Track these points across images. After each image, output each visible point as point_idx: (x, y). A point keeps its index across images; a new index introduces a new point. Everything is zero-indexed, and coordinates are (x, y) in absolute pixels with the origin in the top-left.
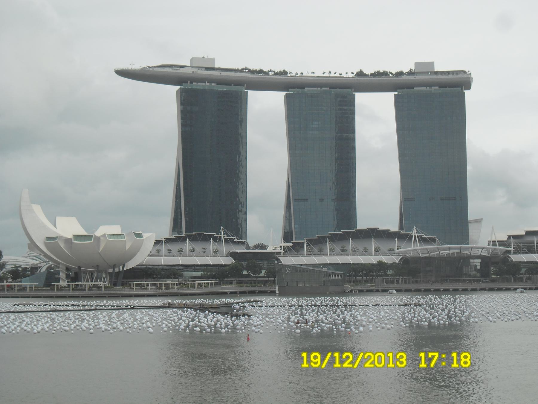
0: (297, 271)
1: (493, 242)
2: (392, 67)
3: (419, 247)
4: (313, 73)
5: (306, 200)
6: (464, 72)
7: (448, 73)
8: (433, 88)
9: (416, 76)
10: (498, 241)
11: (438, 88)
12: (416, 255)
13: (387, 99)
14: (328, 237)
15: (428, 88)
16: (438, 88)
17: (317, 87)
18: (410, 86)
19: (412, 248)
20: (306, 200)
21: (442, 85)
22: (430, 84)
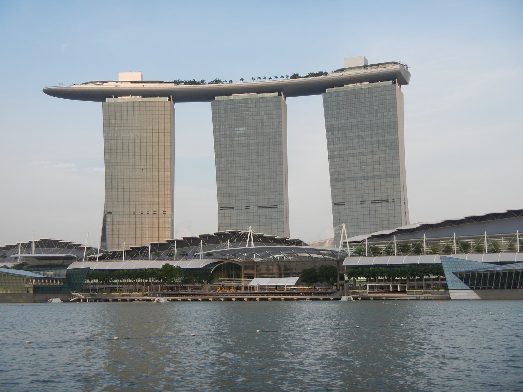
2: (330, 66)
4: (242, 80)
5: (232, 208)
6: (395, 63)
7: (377, 65)
8: (363, 83)
9: (343, 73)
11: (368, 83)
12: (247, 260)
13: (316, 101)
14: (178, 241)
15: (359, 84)
16: (368, 83)
17: (244, 93)
20: (232, 208)
21: (373, 79)
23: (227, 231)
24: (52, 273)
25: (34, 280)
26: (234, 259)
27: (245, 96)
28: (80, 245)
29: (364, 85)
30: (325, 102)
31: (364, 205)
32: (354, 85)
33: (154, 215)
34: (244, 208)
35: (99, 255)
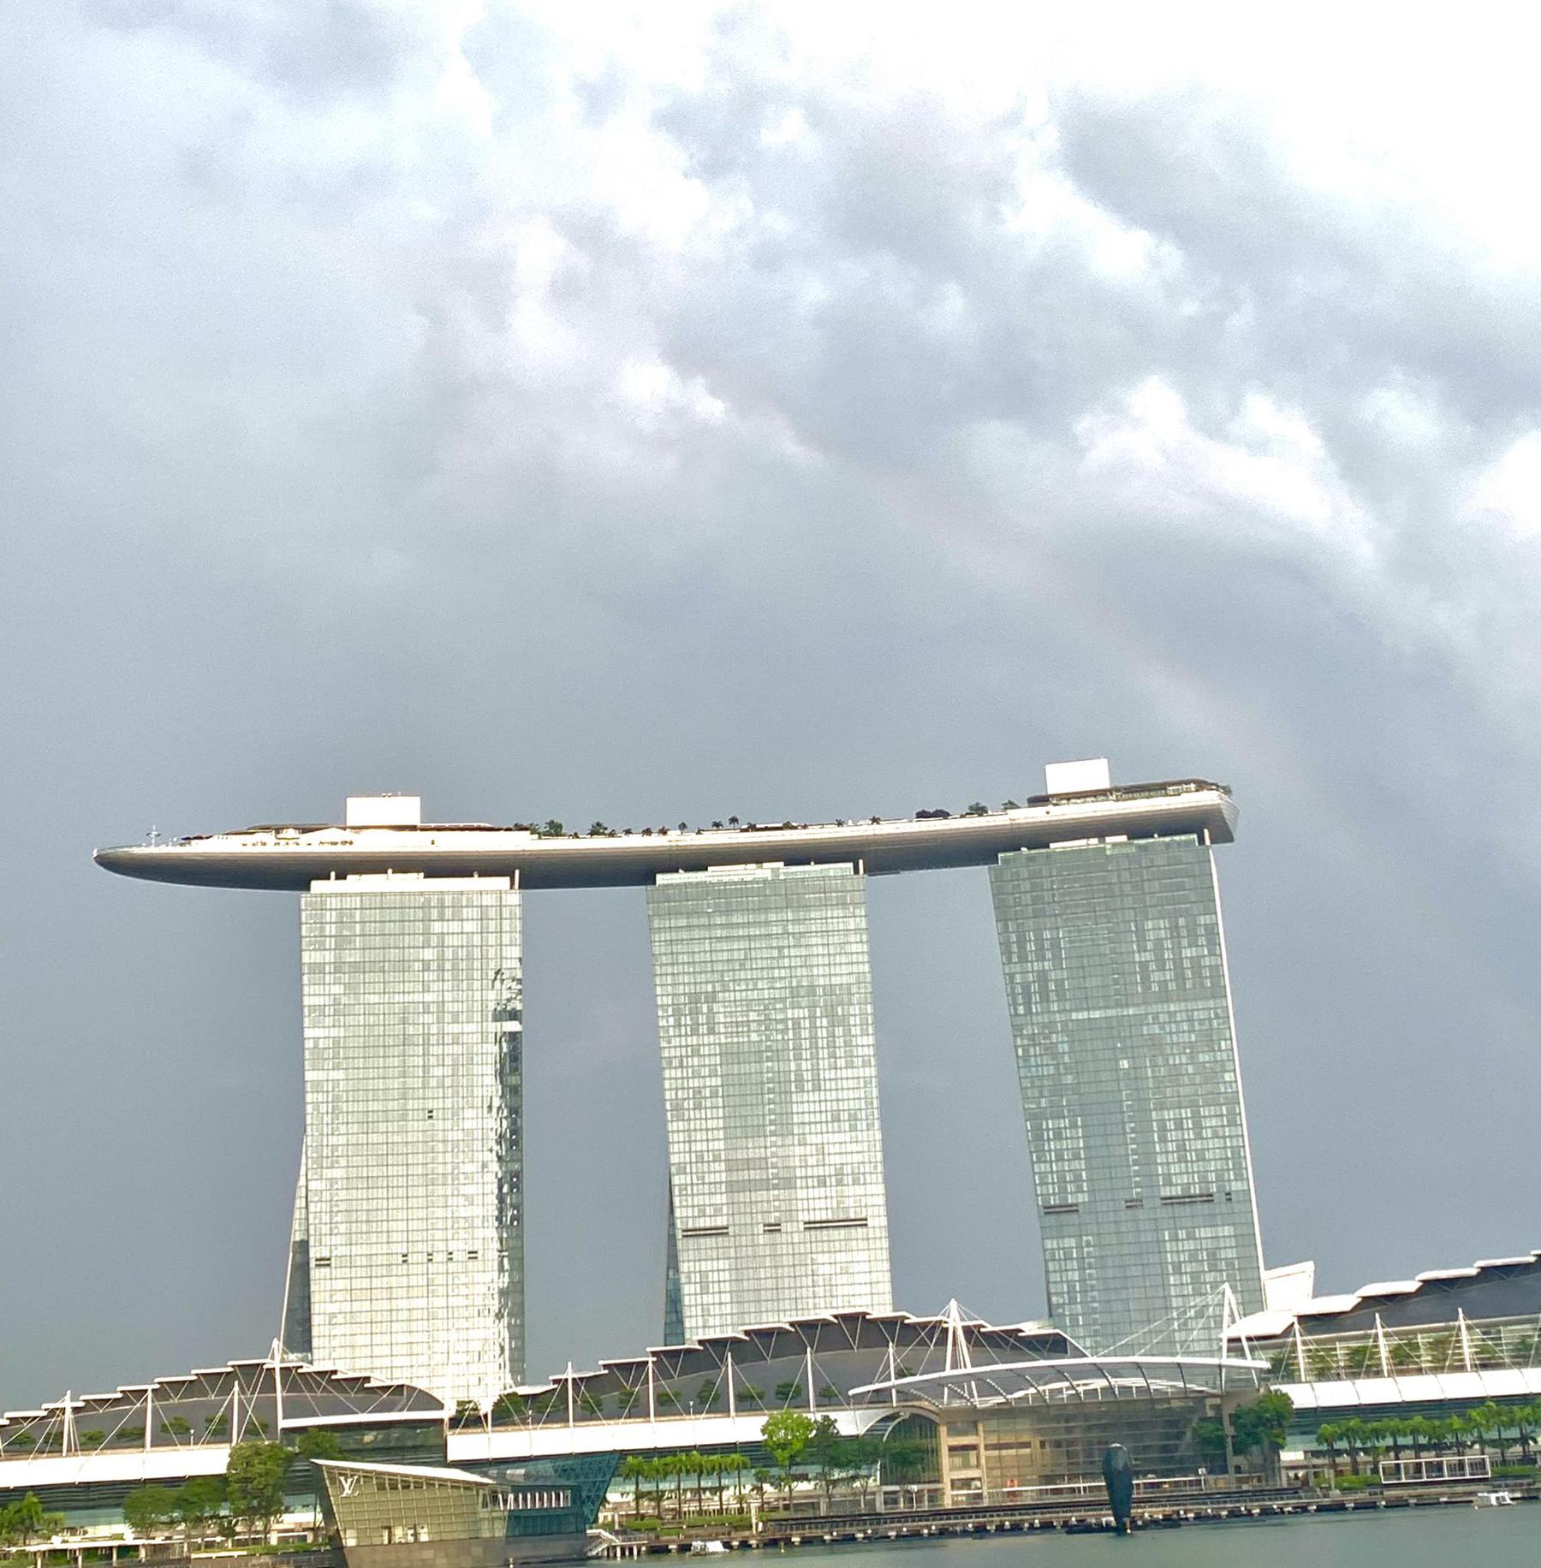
0: (381, 1487)
1: (1230, 1340)
3: (970, 1370)
8: (1109, 839)
10: (1249, 1339)
15: (1094, 841)
16: (1124, 838)
18: (1038, 838)
19: (949, 1372)
22: (1100, 828)
23: (827, 1315)
24: (522, 1471)
25: (511, 1497)
26: (916, 1403)
27: (766, 871)
28: (367, 1379)
29: (1114, 845)
30: (998, 893)
31: (1141, 1214)
32: (1083, 842)
33: (470, 1263)
34: (761, 1228)
35: (486, 1407)
